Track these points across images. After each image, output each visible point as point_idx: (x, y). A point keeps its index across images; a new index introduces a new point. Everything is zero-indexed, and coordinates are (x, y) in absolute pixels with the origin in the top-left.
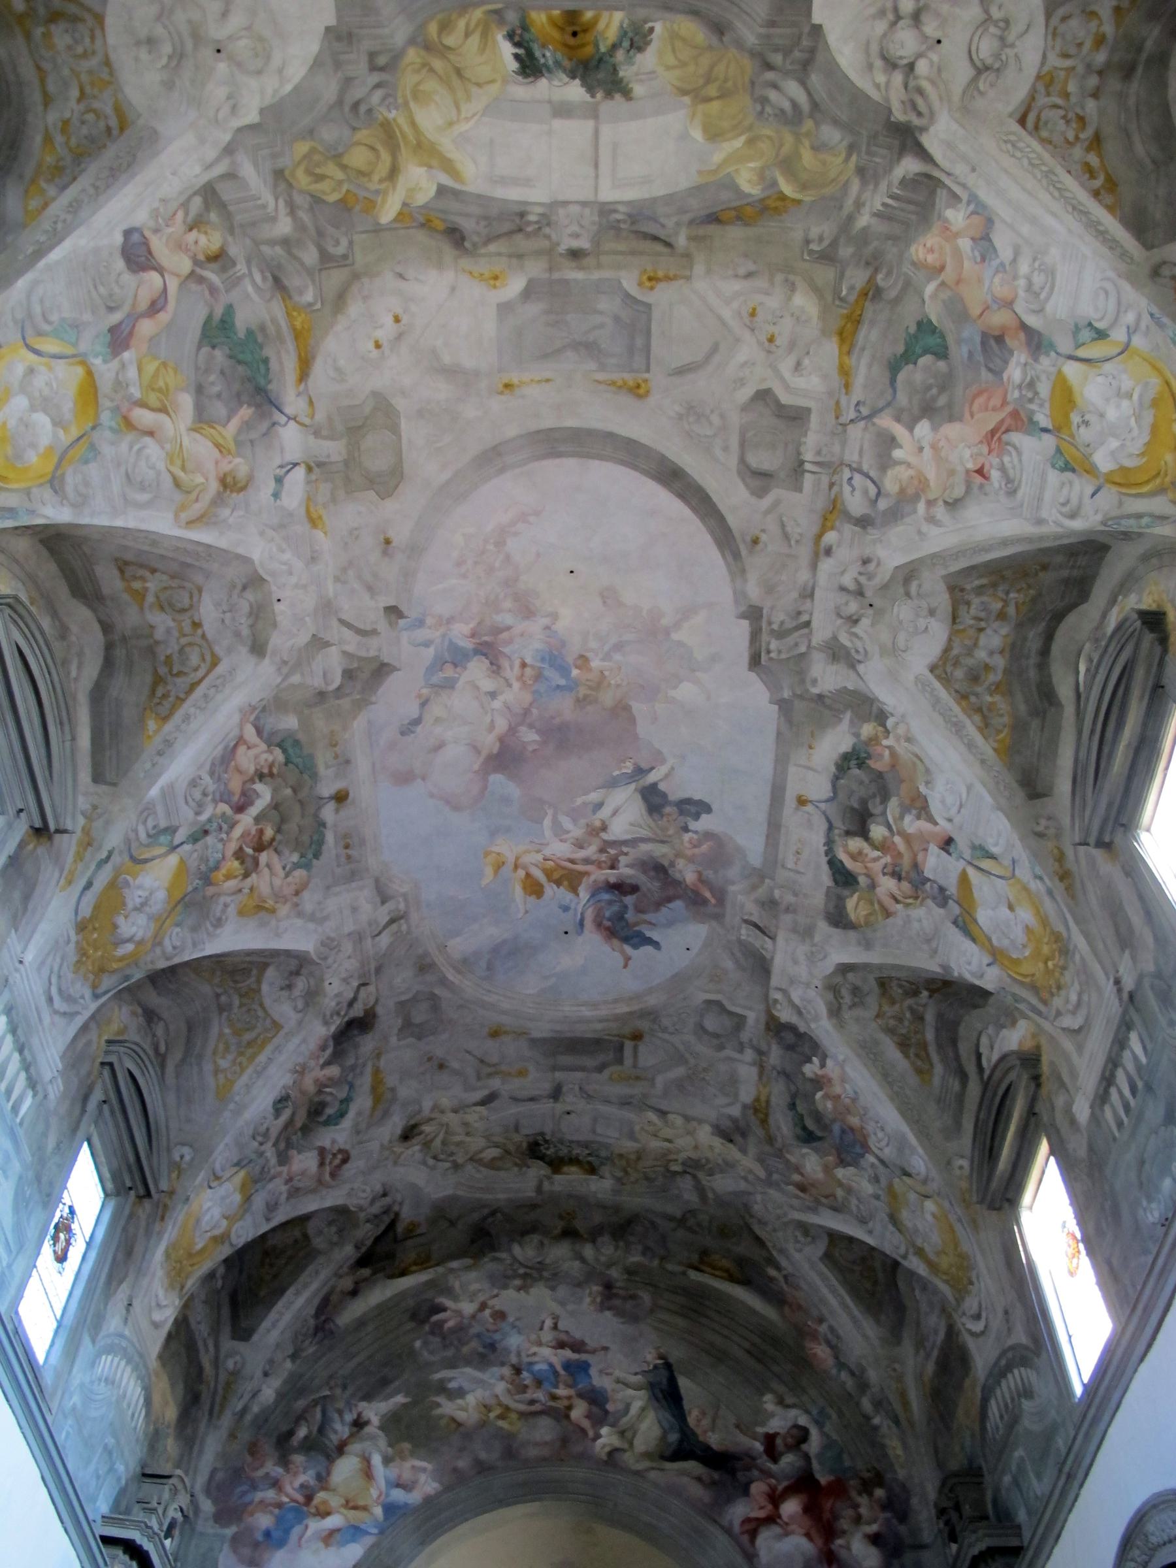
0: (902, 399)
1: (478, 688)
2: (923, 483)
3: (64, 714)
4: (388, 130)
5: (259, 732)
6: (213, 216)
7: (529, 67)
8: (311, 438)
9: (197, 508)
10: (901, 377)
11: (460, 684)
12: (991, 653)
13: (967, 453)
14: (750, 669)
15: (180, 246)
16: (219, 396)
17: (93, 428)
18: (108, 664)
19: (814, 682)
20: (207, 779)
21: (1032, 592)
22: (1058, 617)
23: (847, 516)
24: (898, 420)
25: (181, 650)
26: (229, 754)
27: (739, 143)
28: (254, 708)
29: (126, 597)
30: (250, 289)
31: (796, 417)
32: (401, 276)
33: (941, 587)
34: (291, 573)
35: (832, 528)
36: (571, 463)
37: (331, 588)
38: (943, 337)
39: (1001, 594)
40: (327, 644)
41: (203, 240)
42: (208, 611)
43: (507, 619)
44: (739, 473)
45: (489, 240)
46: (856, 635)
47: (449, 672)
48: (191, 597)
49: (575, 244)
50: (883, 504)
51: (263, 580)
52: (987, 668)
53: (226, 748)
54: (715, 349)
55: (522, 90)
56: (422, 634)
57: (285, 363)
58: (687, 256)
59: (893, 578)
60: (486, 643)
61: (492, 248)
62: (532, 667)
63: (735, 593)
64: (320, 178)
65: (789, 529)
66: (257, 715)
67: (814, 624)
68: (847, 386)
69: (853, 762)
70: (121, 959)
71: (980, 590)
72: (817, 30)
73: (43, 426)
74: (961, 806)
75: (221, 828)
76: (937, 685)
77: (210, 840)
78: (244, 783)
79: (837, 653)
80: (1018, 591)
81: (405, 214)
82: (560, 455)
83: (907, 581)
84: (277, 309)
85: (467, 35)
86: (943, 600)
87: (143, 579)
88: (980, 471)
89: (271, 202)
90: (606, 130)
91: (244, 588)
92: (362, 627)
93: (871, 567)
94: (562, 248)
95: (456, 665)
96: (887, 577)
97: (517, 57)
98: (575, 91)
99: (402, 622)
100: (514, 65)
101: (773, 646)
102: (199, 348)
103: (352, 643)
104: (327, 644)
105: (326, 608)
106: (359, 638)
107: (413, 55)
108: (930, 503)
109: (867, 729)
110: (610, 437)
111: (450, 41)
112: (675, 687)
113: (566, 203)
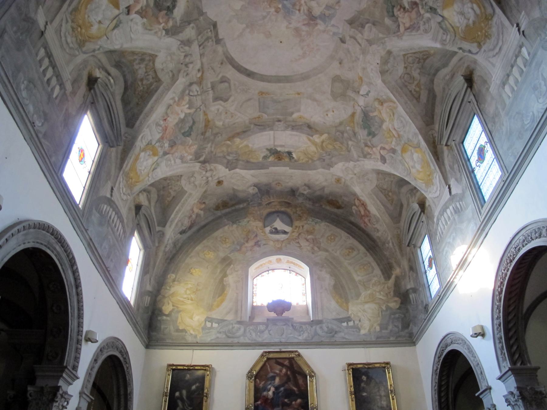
0: (190, 119)
1: (318, 3)
2: (178, 105)
3: (443, 113)
4: (323, 148)
5: (399, 26)
6: (365, 153)
7: (290, 153)
8: (356, 98)
9: (391, 104)
10: (192, 122)
11: (324, 6)
12: (140, 68)
13: (170, 120)
14: (216, 22)
15: (374, 153)
16: (376, 122)
17: (406, 143)
18: (437, 70)
19: (193, 28)
20: (422, 28)
21: (137, 93)
22: (126, 89)
23: (195, 83)
24: (190, 113)
25: (413, 63)
26: (412, 28)
27: (240, 146)
28: (398, 36)
29: (422, 87)
30: (362, 137)
31: (216, 99)
32: (324, 123)
33: (163, 79)
34: (372, 69)
35: (199, 78)
36: (281, 74)
37: (361, 57)
38: (185, 136)
39: (145, 86)
40: (367, 40)
41: (369, 151)
42: (400, 70)
43: (304, 28)
44: (229, 79)
45: (302, 125)
46: (183, 52)
47: (327, 13)
48: (404, 77)
49: (279, 123)
50: (187, 92)
51: (380, 73)
52: (139, 64)
53: (411, 31)
54: (241, 106)
55: (291, 150)
56: (335, 30)
57: (358, 117)
58: (250, 123)
59: (178, 76)
60: (313, 20)
61: (301, 124)
62: (296, 10)
63: (226, 46)
64: (340, 147)
65: (212, 71)
66: (396, 33)
67: (198, 47)
68: (204, 112)
69: (171, 7)
70: (480, 8)
71: (151, 84)
72: (227, 168)
73: (415, 156)
74: (131, 30)
75: (426, 4)
76: (153, 53)
77: (431, 4)
78: (411, 12)
79: (187, 43)
80: (141, 90)
81: (322, 134)
82: (285, 76)
83: (173, 75)
84: (356, 129)
85: (303, 159)
86: (161, 75)
87: (415, 91)
88: (165, 120)
89: (352, 148)
90: (272, 143)
91: (387, 71)
92: (355, 41)
93: (185, 74)
94: (283, 122)
95: (324, 14)
96: (180, 75)
97: (292, 155)
98: (279, 149)
99: (341, 36)
100: (293, 154)
101: (210, 33)
102: (378, 134)
103: (359, 36)
104: (367, 40)
105: (364, 52)
106: (357, 37)
107: (315, 159)
108: (175, 102)
109: (170, 24)
110: (269, 82)
111: (307, 159)
112: (242, 6)
113: (282, 130)
